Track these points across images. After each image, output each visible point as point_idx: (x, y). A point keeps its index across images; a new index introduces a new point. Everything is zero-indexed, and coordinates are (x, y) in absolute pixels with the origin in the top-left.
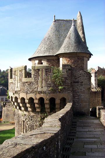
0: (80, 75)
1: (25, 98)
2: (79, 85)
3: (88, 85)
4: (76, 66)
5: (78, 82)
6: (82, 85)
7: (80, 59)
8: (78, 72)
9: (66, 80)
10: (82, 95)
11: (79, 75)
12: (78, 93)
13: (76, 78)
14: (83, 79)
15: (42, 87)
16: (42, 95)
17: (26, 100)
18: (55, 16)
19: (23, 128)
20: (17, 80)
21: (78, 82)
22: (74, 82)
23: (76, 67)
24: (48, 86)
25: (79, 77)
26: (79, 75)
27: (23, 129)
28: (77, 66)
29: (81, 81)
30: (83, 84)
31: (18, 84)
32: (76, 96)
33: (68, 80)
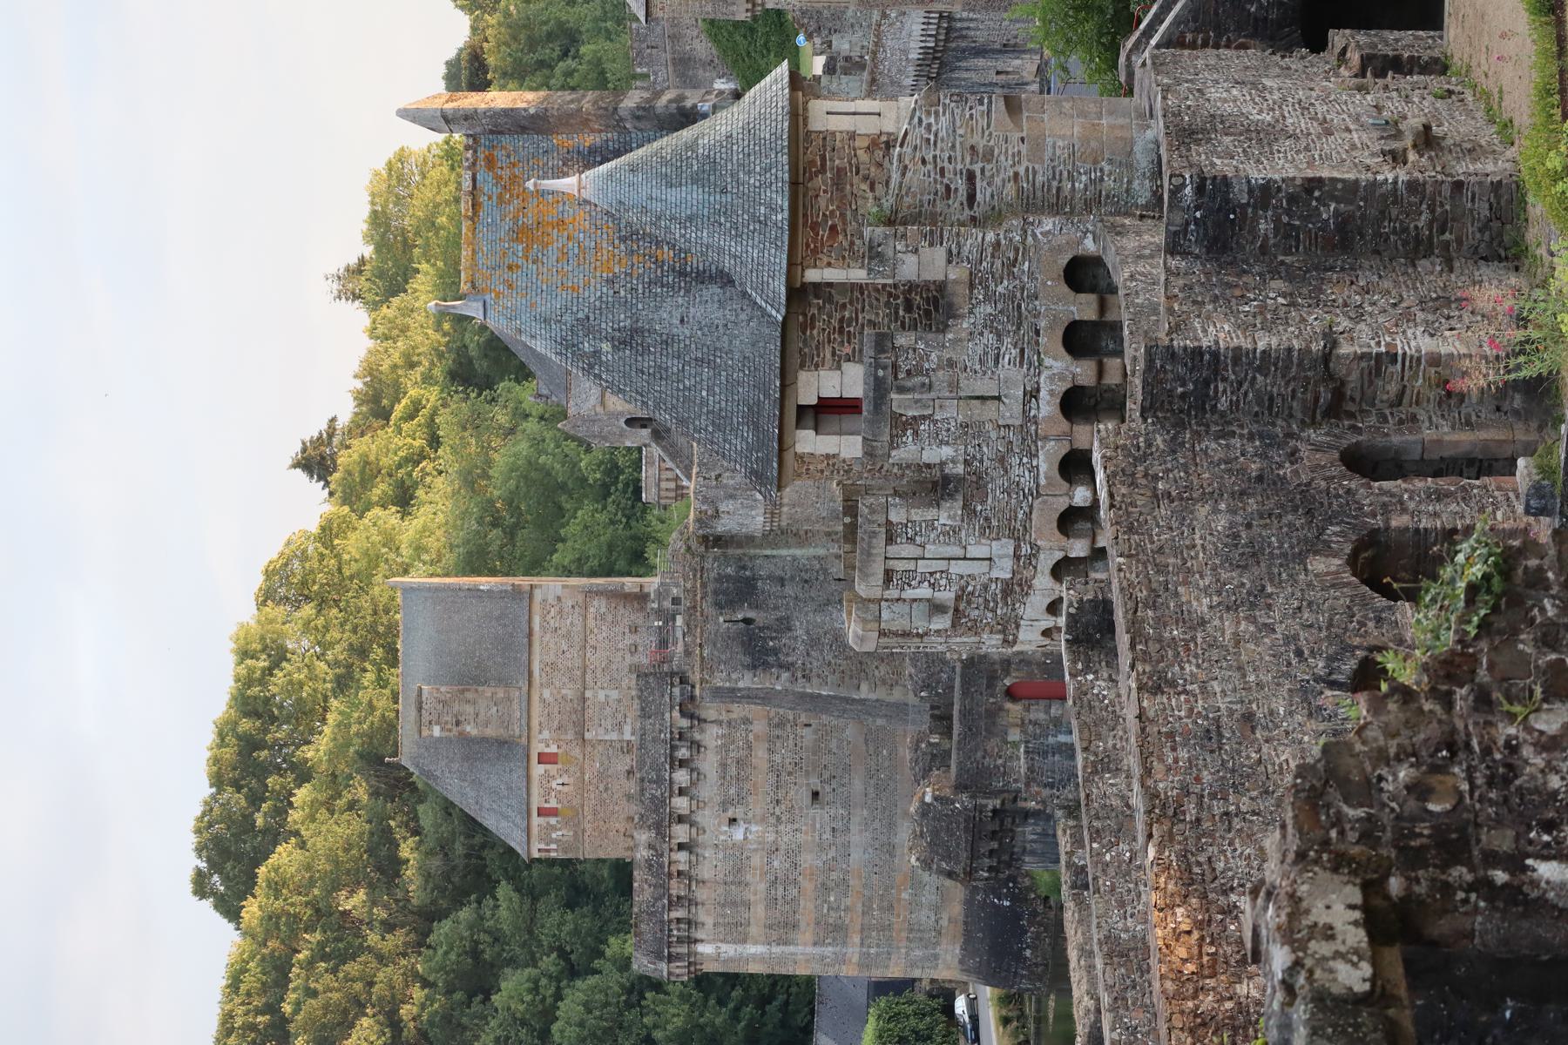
1: (1062, 504)
2: (987, 174)
3: (989, 111)
4: (865, 187)
5: (971, 177)
6: (989, 155)
7: (823, 158)
11: (930, 167)
12: (1040, 179)
13: (948, 188)
14: (953, 146)
15: (998, 398)
16: (1047, 407)
20: (942, 565)
21: (971, 177)
22: (971, 198)
23: (872, 189)
24: (997, 361)
25: (942, 169)
26: (930, 167)
28: (866, 178)
31: (973, 551)
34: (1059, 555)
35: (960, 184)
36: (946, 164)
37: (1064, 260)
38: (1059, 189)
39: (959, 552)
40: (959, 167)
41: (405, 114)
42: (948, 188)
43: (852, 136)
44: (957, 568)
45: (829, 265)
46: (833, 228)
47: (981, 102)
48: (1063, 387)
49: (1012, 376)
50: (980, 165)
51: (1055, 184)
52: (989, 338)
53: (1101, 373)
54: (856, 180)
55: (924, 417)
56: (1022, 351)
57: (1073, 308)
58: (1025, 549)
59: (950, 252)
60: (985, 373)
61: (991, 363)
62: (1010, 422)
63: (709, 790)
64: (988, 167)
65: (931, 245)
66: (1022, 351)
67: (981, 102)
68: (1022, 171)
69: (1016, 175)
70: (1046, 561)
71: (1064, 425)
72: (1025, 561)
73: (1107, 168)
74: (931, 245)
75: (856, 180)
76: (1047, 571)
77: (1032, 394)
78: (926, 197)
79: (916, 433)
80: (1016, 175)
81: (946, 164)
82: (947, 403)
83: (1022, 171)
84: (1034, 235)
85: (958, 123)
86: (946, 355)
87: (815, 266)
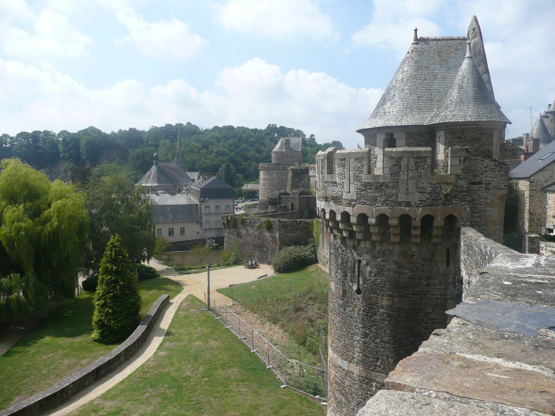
0: (485, 167)
2: (481, 189)
3: (502, 189)
5: (480, 183)
8: (481, 162)
9: (459, 180)
10: (488, 209)
11: (484, 169)
12: (479, 206)
13: (477, 176)
14: (490, 177)
17: (369, 220)
18: (416, 30)
19: (357, 274)
20: (347, 177)
21: (480, 183)
23: (475, 151)
24: (419, 192)
25: (483, 174)
27: (357, 277)
28: (478, 148)
29: (486, 180)
30: (491, 186)
32: (475, 212)
33: (461, 179)
34: (351, 214)
35: (478, 179)
36: (484, 175)
37: (456, 215)
38: (475, 212)
39: (352, 182)
40: (484, 179)
41: (476, 20)
42: (477, 176)
43: (492, 144)
44: (346, 181)
45: (446, 138)
46: (461, 138)
47: (505, 186)
48: (412, 215)
49: (415, 198)
50: (484, 186)
51: (477, 211)
52: (429, 190)
53: (415, 228)
54: (478, 145)
55: (401, 168)
56: (425, 201)
57: (439, 218)
58: (353, 203)
59: (460, 176)
60: (417, 188)
61: (420, 190)
62: (399, 197)
63: (279, 171)
64: (483, 189)
65: (462, 169)
66: (425, 201)
67: (505, 186)
68: (482, 200)
69: (481, 198)
70: (348, 209)
71: (398, 215)
72: (350, 203)
73: (482, 228)
74: (462, 169)
75: (478, 145)
76: (346, 210)
77: (408, 204)
78: (473, 168)
79: (394, 165)
80: (481, 198)
81: (484, 175)
82: (406, 175)
83: (482, 200)
84: (465, 204)
85: (498, 179)
86: (423, 175)
87: (445, 133)
